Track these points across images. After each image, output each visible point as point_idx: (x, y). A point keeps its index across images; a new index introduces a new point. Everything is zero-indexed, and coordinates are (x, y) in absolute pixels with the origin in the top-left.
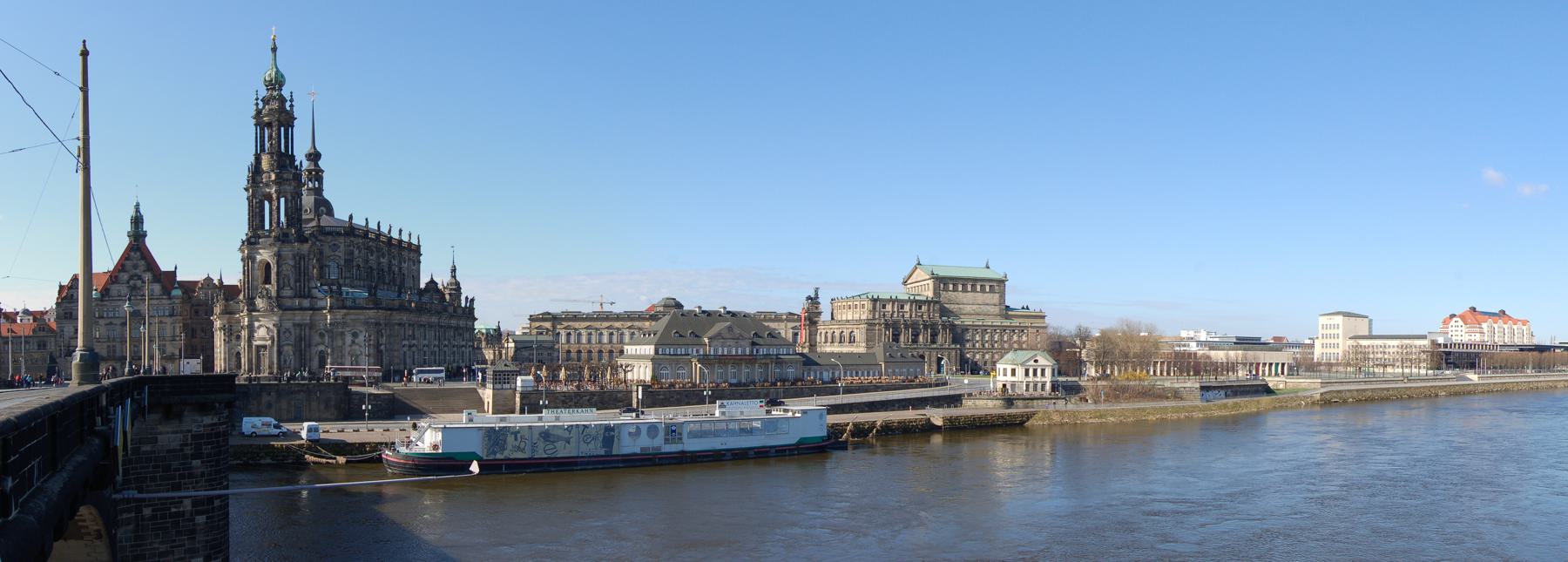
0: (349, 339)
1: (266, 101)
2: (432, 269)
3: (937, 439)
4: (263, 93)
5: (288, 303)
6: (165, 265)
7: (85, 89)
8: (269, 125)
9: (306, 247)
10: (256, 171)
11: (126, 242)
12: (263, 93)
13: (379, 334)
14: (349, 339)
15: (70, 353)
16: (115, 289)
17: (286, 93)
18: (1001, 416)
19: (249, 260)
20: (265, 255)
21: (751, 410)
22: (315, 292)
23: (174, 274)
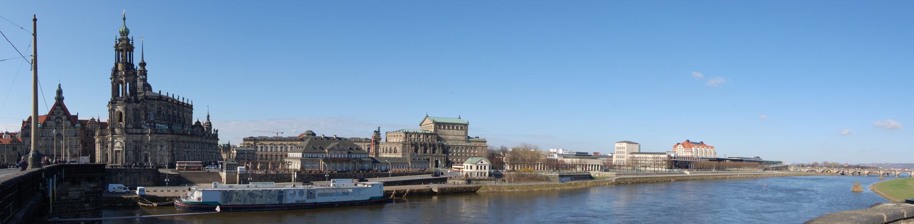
0: (159, 148)
1: (120, 40)
2: (198, 116)
3: (435, 198)
4: (119, 37)
5: (130, 131)
6: (72, 113)
7: (35, 34)
8: (122, 50)
9: (139, 105)
10: (116, 70)
11: (54, 102)
12: (119, 37)
13: (173, 146)
14: (159, 148)
15: (28, 152)
16: (49, 123)
17: (130, 37)
18: (465, 188)
19: (112, 111)
20: (119, 108)
21: (348, 184)
22: (143, 126)
23: (76, 116)
